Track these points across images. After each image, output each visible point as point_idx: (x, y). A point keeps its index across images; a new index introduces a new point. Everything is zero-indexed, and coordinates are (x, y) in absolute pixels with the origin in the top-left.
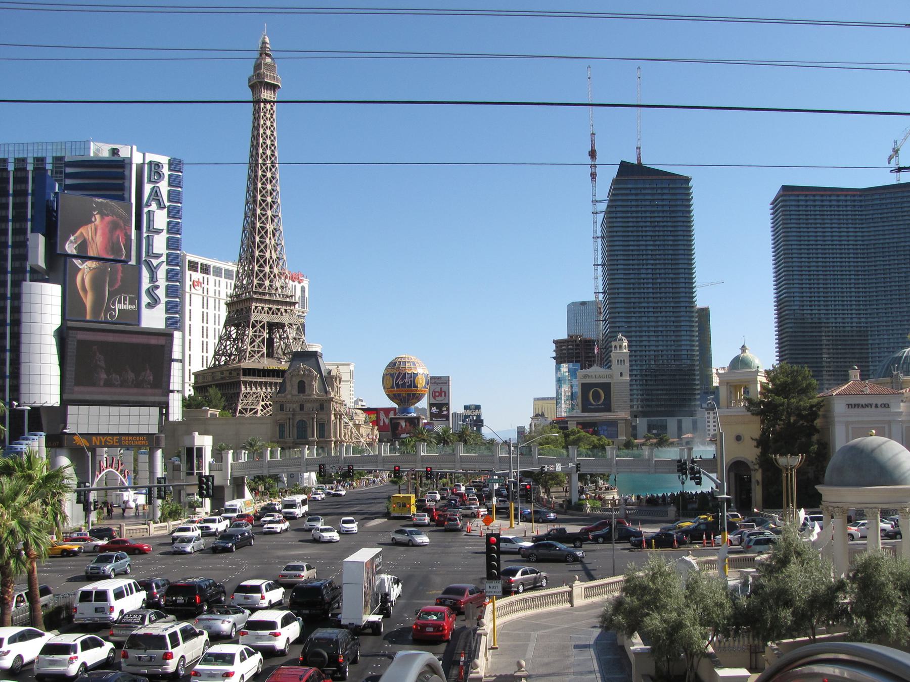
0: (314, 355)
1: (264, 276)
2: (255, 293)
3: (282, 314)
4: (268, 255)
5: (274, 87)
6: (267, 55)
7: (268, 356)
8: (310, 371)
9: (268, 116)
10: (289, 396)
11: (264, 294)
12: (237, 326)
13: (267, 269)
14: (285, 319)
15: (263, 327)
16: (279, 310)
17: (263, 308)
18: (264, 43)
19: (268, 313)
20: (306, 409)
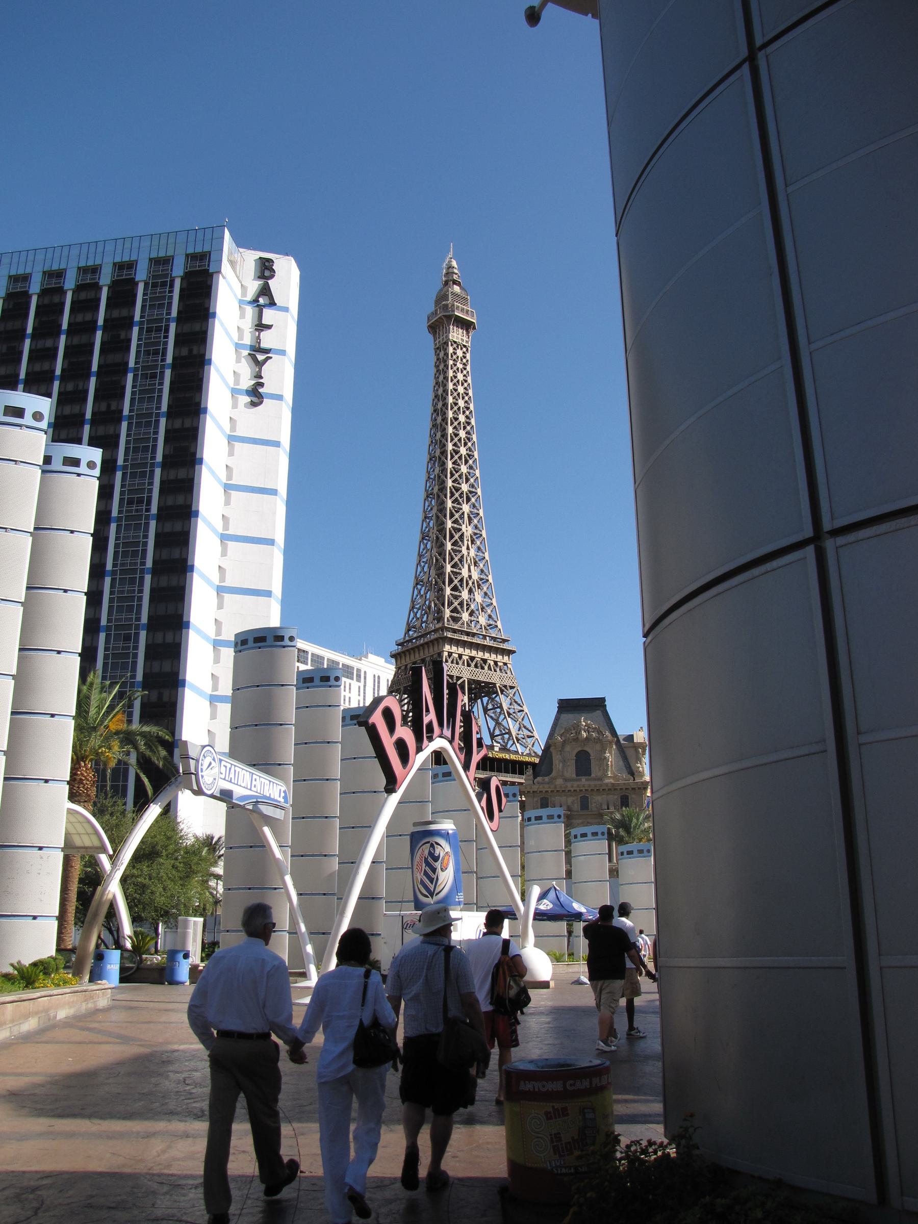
0: (597, 705)
1: (461, 604)
2: (448, 629)
4: (465, 573)
5: (466, 325)
6: (455, 282)
8: (600, 732)
10: (559, 782)
11: (462, 632)
13: (465, 595)
14: (496, 678)
16: (485, 661)
17: (460, 656)
18: (450, 267)
19: (469, 665)
20: (593, 806)
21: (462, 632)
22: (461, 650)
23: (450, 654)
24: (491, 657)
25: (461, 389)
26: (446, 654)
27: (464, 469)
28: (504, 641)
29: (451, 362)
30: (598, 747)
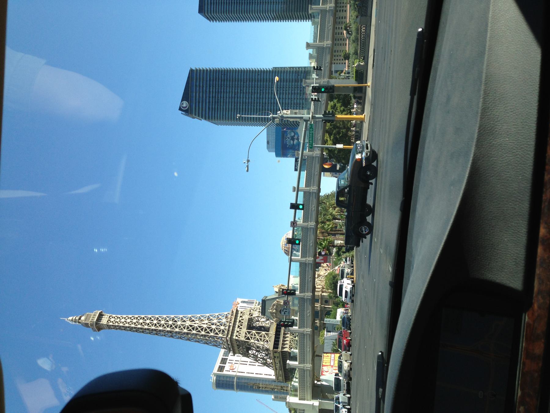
0: (264, 303)
3: (243, 320)
4: (205, 326)
5: (101, 316)
6: (80, 319)
7: (268, 331)
8: (274, 305)
9: (118, 320)
11: (228, 330)
12: (249, 349)
14: (246, 317)
15: (249, 333)
16: (240, 321)
17: (238, 332)
18: (72, 320)
19: (241, 328)
21: (228, 330)
22: (236, 331)
23: (237, 336)
24: (239, 318)
25: (129, 320)
26: (236, 338)
27: (163, 322)
28: (233, 312)
29: (117, 324)
30: (279, 306)
